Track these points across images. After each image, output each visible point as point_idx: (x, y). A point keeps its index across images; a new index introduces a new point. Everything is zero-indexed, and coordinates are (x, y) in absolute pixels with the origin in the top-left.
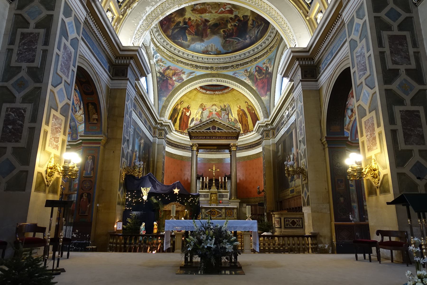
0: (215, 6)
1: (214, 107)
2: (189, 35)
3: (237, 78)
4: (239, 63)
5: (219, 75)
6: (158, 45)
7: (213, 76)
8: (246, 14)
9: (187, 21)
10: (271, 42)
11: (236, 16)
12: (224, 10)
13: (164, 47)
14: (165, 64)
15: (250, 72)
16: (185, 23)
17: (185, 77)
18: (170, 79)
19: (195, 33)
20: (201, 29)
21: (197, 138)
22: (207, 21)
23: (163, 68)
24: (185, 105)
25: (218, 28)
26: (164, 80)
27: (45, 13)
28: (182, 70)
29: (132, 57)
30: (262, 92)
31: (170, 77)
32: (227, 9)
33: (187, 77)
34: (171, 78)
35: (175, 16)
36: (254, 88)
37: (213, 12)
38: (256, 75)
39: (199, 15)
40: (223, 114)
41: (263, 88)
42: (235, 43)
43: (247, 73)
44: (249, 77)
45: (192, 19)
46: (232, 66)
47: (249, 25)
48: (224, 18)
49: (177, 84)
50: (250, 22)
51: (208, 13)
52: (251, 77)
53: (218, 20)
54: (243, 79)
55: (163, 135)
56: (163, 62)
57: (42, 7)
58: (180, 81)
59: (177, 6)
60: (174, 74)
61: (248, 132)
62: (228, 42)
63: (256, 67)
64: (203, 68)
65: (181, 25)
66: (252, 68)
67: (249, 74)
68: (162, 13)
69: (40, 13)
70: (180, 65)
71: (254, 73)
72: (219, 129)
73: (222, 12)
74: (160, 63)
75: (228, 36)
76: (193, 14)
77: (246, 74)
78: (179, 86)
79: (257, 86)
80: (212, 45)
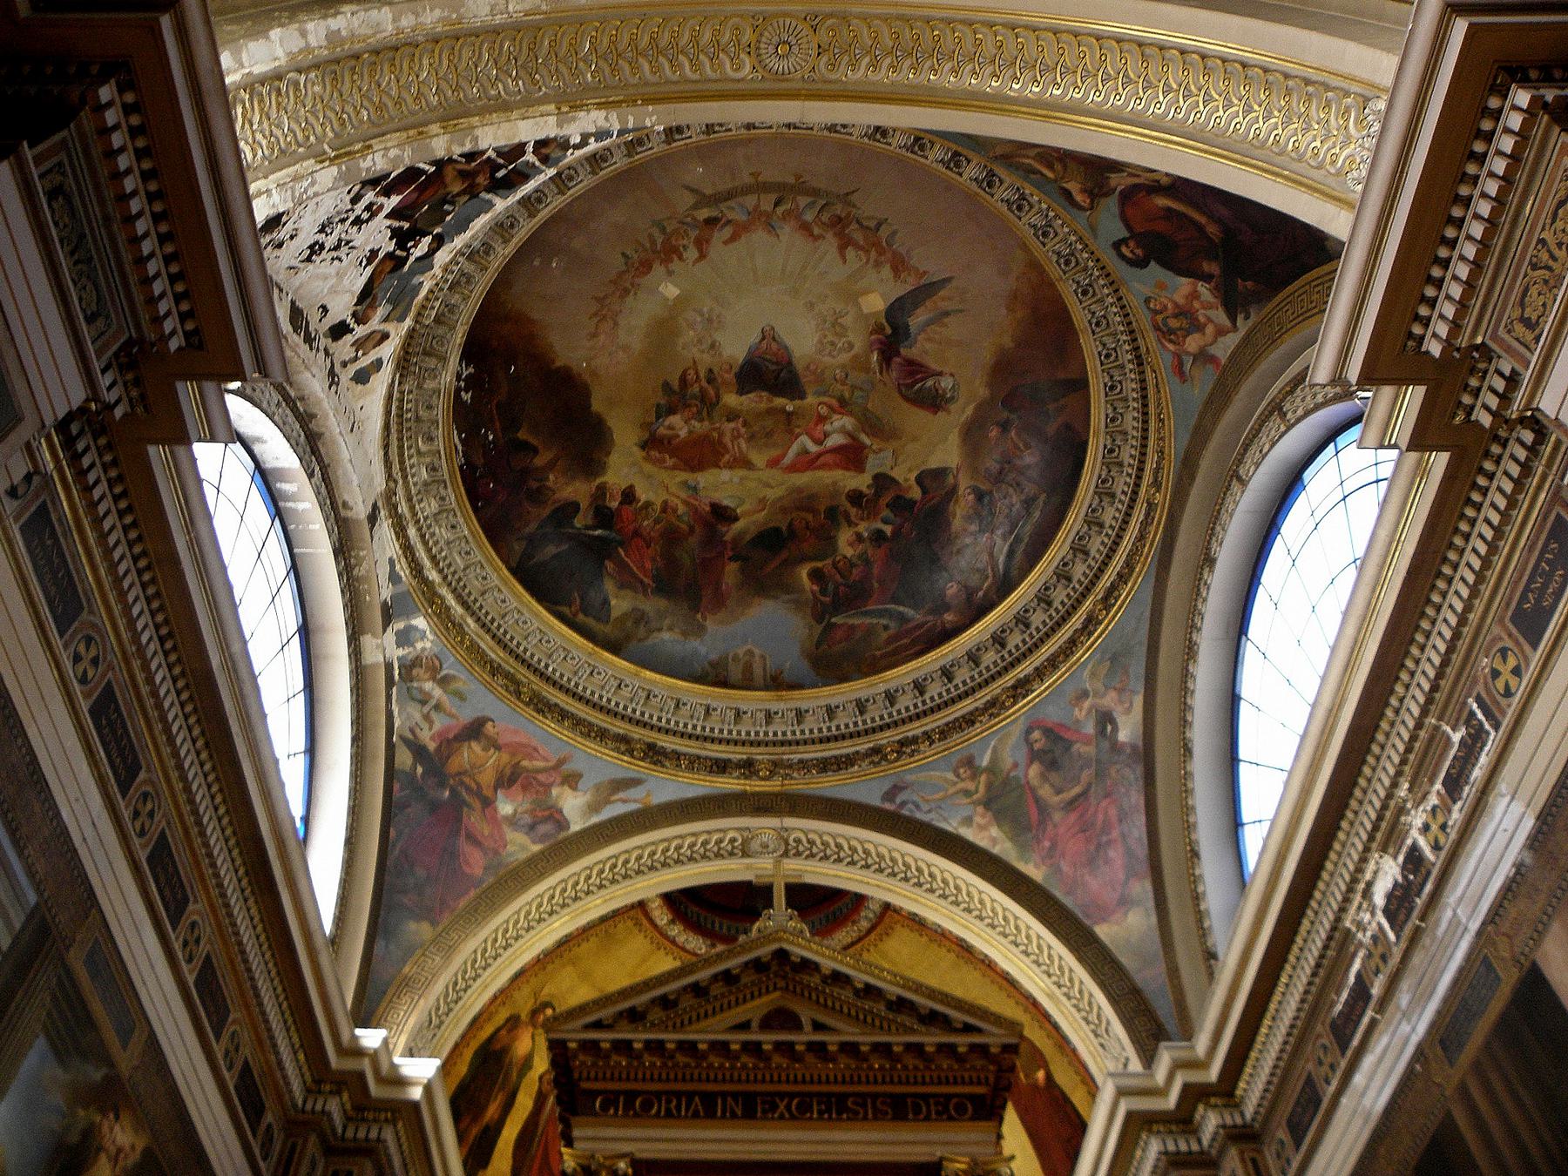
0: (769, 423)
2: (622, 586)
3: (910, 821)
4: (915, 729)
6: (433, 575)
8: (933, 463)
9: (614, 505)
10: (1105, 564)
11: (883, 481)
12: (813, 448)
13: (465, 604)
14: (460, 696)
15: (992, 770)
16: (604, 516)
17: (574, 806)
18: (477, 805)
19: (655, 579)
20: (687, 560)
21: (634, 1106)
22: (722, 514)
23: (439, 722)
25: (784, 555)
26: (435, 807)
28: (561, 762)
31: (478, 793)
32: (835, 440)
33: (594, 808)
34: (488, 803)
35: (551, 466)
37: (759, 459)
38: (1035, 782)
39: (682, 476)
42: (884, 635)
43: (974, 777)
44: (988, 803)
45: (643, 495)
46: (876, 751)
47: (957, 523)
48: (813, 497)
50: (960, 511)
51: (730, 466)
53: (784, 510)
54: (952, 825)
56: (444, 682)
58: (544, 828)
59: (552, 107)
60: (509, 779)
62: (839, 634)
63: (1029, 731)
64: (695, 763)
65: (579, 522)
66: (1002, 743)
67: (989, 786)
68: (453, 115)
70: (550, 726)
71: (1019, 773)
73: (808, 462)
74: (428, 686)
75: (842, 595)
76: (648, 467)
77: (970, 786)
78: (532, 861)
80: (750, 653)
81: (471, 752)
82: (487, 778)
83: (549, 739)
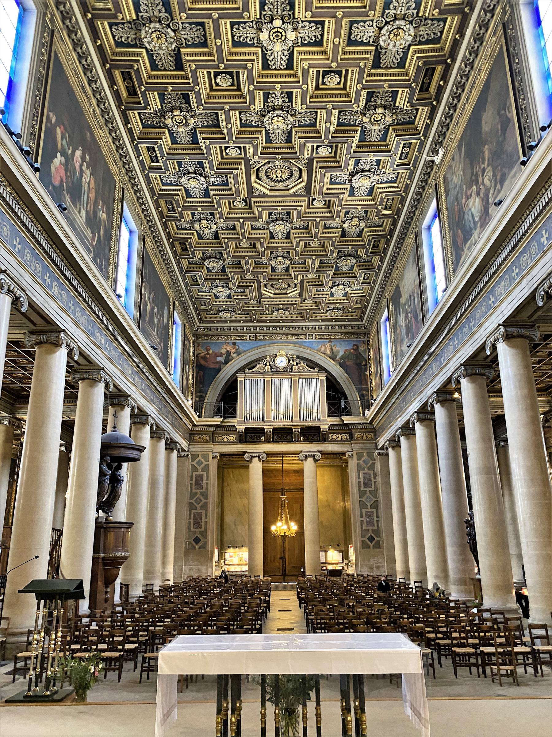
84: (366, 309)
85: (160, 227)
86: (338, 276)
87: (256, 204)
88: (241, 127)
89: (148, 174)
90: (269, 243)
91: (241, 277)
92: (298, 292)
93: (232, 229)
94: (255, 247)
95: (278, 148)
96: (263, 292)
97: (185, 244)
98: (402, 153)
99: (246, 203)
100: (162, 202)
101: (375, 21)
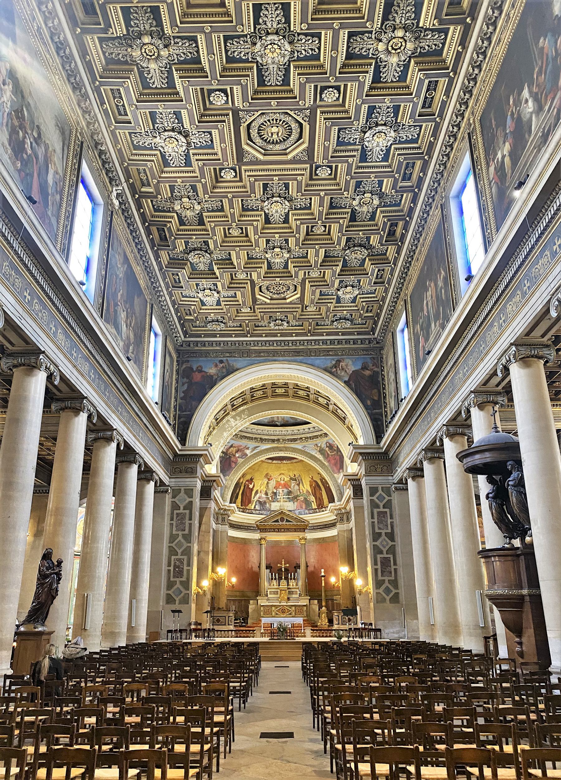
1: (283, 476)
4: (308, 435)
5: (286, 449)
7: (280, 450)
17: (248, 452)
24: (248, 477)
27: (189, 500)
29: (214, 481)
30: (335, 469)
34: (234, 456)
36: (326, 464)
40: (293, 485)
41: (335, 465)
46: (301, 438)
49: (240, 460)
52: (321, 451)
54: (313, 453)
55: (226, 521)
57: (186, 497)
60: (237, 452)
61: (322, 507)
64: (268, 440)
69: (185, 500)
72: (287, 521)
78: (242, 463)
79: (329, 461)
81: (230, 450)
82: (234, 452)
83: (244, 443)
84: (379, 319)
85: (142, 231)
86: (347, 273)
87: (247, 173)
88: (227, 62)
89: (127, 166)
90: (263, 228)
91: (237, 310)
92: (305, 145)
93: (228, 260)
94: (247, 236)
95: (275, 91)
96: (245, 147)
97: (178, 275)
98: (426, 98)
99: (236, 172)
100: (154, 229)
101: (374, 32)
